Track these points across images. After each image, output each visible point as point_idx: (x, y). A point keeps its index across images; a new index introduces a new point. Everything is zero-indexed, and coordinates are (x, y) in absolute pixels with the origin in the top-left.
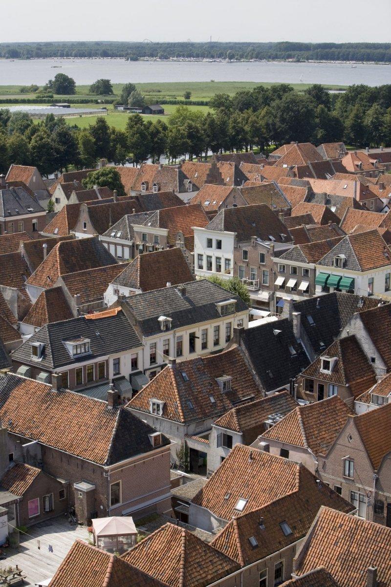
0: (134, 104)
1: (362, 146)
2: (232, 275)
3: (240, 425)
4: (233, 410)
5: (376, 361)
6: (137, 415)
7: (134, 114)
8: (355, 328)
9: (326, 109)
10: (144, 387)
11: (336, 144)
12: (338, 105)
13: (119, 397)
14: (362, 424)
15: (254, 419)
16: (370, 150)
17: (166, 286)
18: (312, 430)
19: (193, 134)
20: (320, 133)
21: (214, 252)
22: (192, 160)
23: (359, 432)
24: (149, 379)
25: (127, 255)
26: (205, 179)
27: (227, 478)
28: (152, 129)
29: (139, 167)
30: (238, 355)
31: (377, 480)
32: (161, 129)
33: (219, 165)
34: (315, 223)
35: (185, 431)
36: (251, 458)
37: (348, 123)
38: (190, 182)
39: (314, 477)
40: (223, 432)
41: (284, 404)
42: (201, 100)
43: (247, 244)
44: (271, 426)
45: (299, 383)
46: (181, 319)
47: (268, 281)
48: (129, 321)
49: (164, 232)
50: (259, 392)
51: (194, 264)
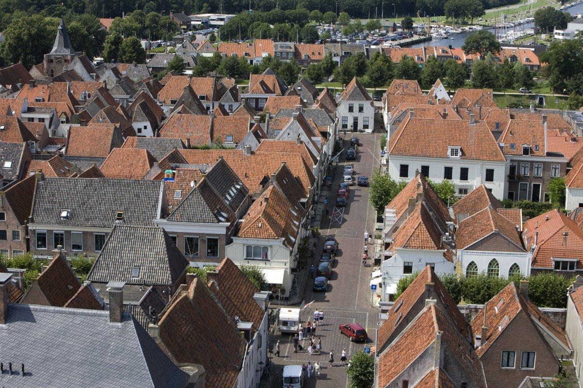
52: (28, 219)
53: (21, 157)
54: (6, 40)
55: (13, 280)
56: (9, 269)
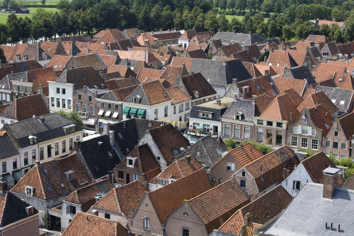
0: (11, 8)
1: (149, 30)
2: (72, 109)
3: (80, 200)
4: (75, 191)
5: (160, 159)
6: (18, 196)
7: (11, 14)
8: (147, 139)
9: (127, 8)
10: (21, 179)
11: (133, 29)
12: (134, 6)
13: (6, 186)
14: (154, 197)
15: (89, 196)
16: (154, 33)
17: (32, 117)
18: (123, 202)
19: (47, 25)
20: (123, 23)
21: (61, 96)
22: (46, 41)
23: (152, 202)
24: (24, 174)
25: (8, 99)
26: (54, 52)
27: (73, 232)
28: (22, 22)
29: (14, 45)
30: (77, 157)
31: (164, 230)
32: (27, 22)
33: (63, 43)
34: (121, 77)
35: (47, 204)
36: (88, 220)
37: (140, 16)
38: (46, 54)
39: (126, 230)
40: (70, 205)
41: (106, 187)
42: (51, 4)
43: (81, 91)
44: (98, 200)
45: (114, 174)
46: (42, 137)
47: (94, 112)
48: (11, 139)
49: (30, 85)
50: (91, 179)
51: (49, 103)
52: (352, 137)
53: (351, 99)
54: (346, 27)
55: (339, 173)
56: (337, 166)
